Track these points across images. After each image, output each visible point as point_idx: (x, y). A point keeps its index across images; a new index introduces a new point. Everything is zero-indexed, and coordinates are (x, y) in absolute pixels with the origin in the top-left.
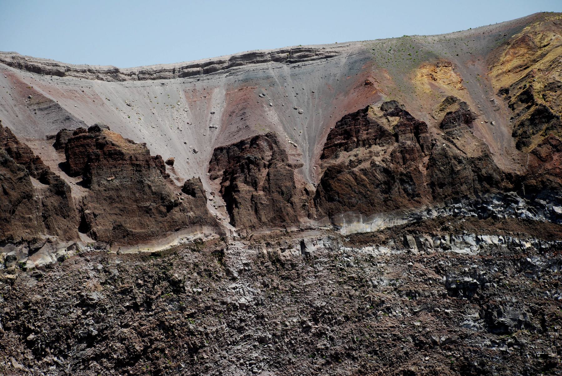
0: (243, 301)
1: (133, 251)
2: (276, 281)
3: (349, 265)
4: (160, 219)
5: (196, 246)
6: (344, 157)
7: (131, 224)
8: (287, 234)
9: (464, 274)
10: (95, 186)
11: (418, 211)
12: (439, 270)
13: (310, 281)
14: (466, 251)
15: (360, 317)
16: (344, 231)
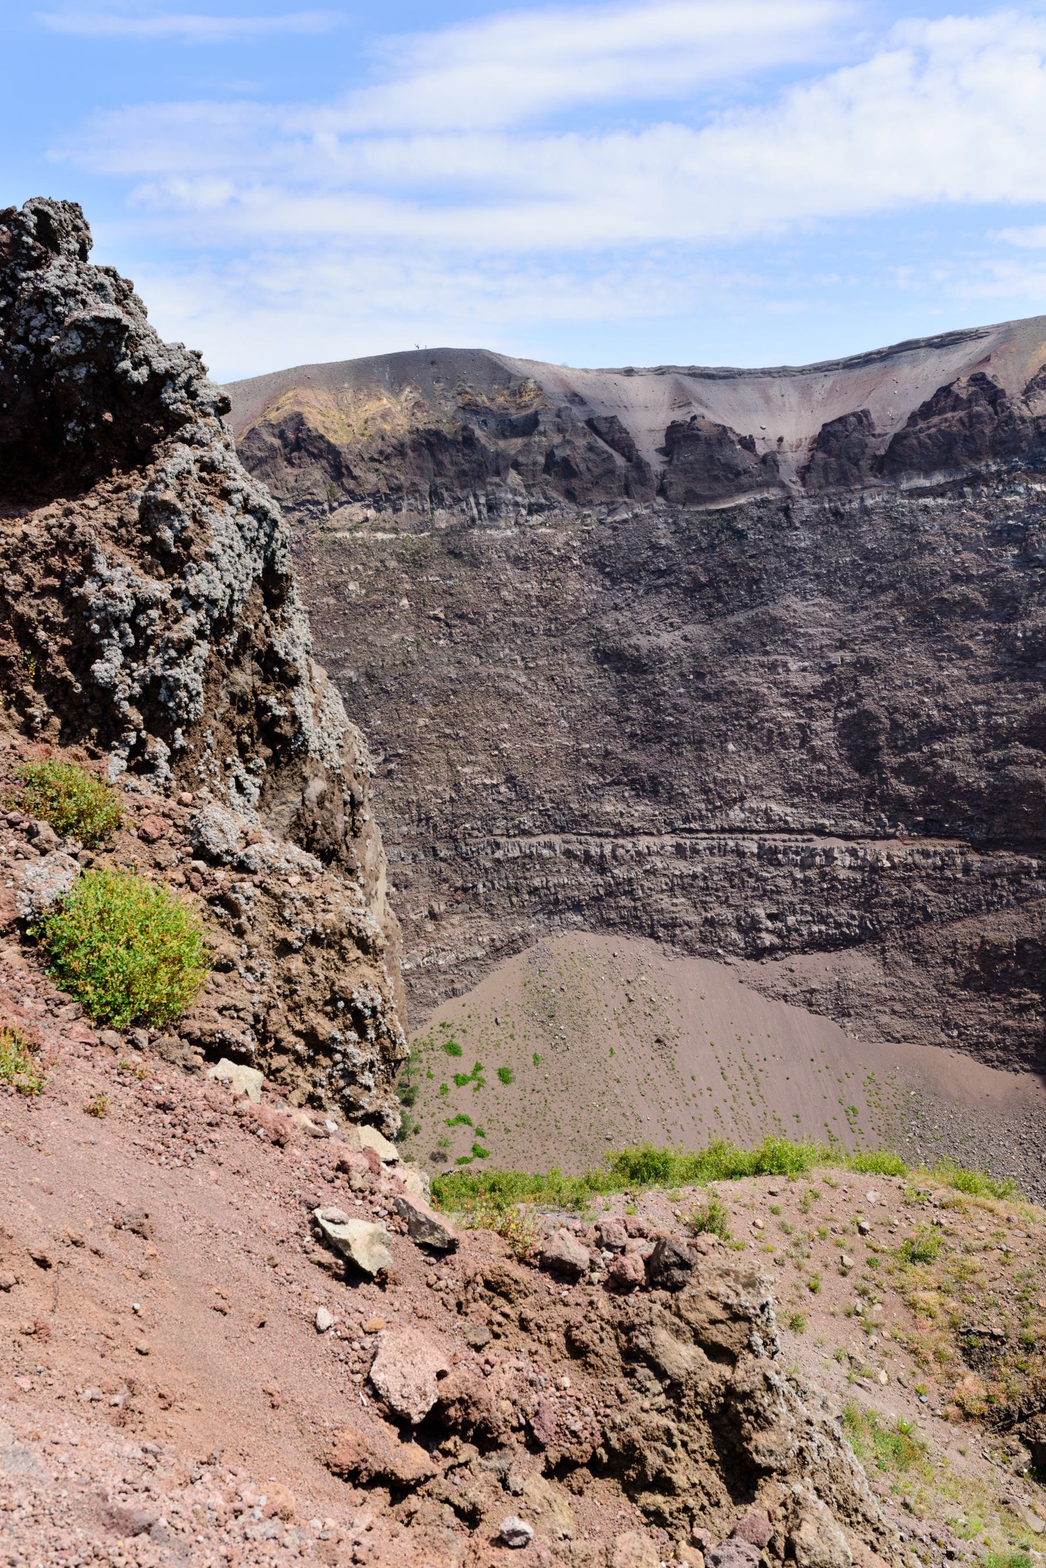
0: (803, 545)
1: (701, 508)
2: (836, 529)
3: (903, 515)
4: (726, 483)
5: (764, 503)
6: (922, 425)
7: (700, 489)
8: (851, 491)
9: (1008, 518)
10: (675, 462)
11: (977, 467)
12: (989, 516)
13: (865, 528)
14: (1017, 498)
15: (906, 556)
16: (905, 486)
